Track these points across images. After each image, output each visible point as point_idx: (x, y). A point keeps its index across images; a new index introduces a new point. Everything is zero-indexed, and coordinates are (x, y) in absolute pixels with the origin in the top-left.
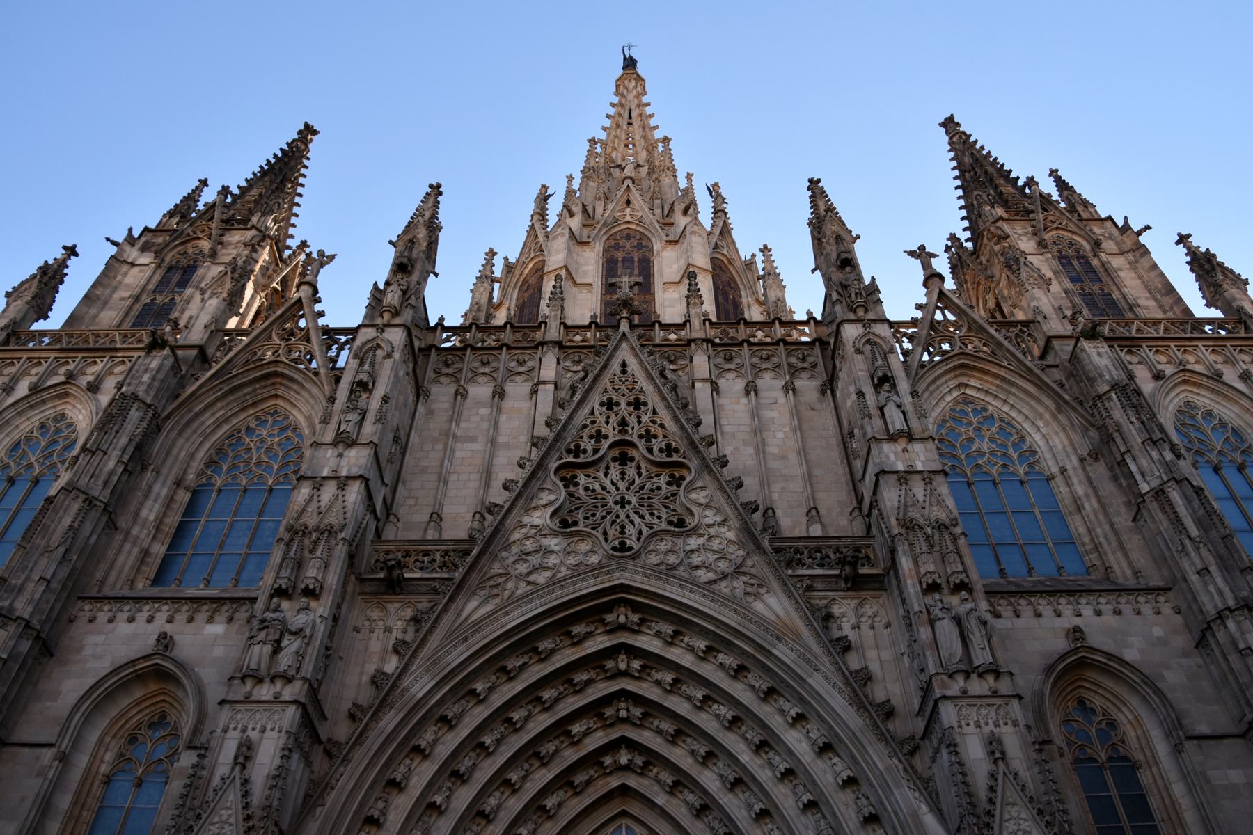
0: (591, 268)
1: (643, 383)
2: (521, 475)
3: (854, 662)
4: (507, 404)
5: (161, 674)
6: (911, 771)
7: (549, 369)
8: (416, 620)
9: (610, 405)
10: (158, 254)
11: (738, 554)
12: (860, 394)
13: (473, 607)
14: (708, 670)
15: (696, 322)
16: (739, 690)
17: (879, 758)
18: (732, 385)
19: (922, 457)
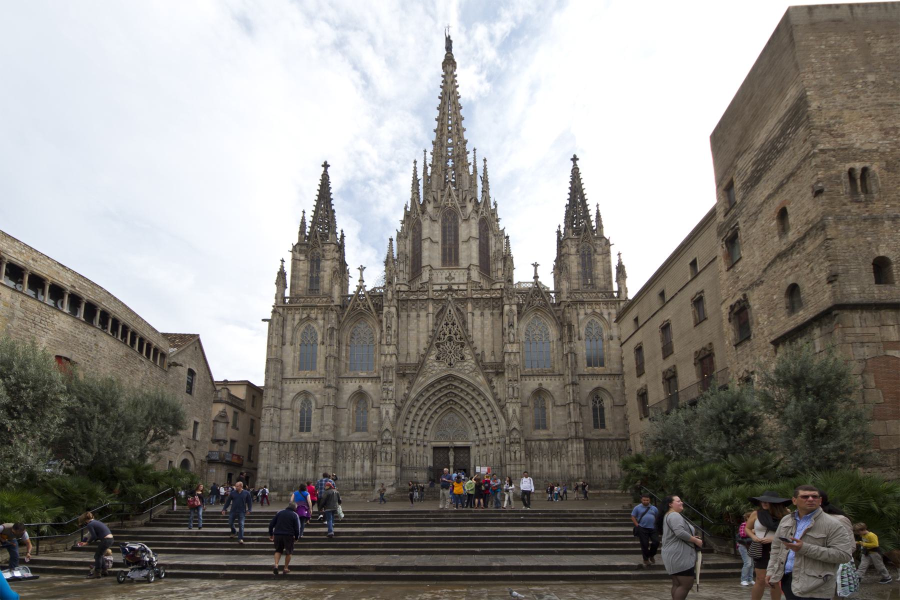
0: (437, 233)
1: (455, 318)
2: (426, 346)
3: (495, 391)
4: (421, 319)
5: (361, 393)
6: (501, 411)
7: (431, 310)
8: (410, 382)
9: (447, 324)
10: (306, 256)
11: (474, 366)
12: (503, 329)
13: (421, 379)
14: (467, 390)
15: (469, 290)
16: (474, 394)
17: (496, 409)
18: (477, 312)
19: (514, 348)
